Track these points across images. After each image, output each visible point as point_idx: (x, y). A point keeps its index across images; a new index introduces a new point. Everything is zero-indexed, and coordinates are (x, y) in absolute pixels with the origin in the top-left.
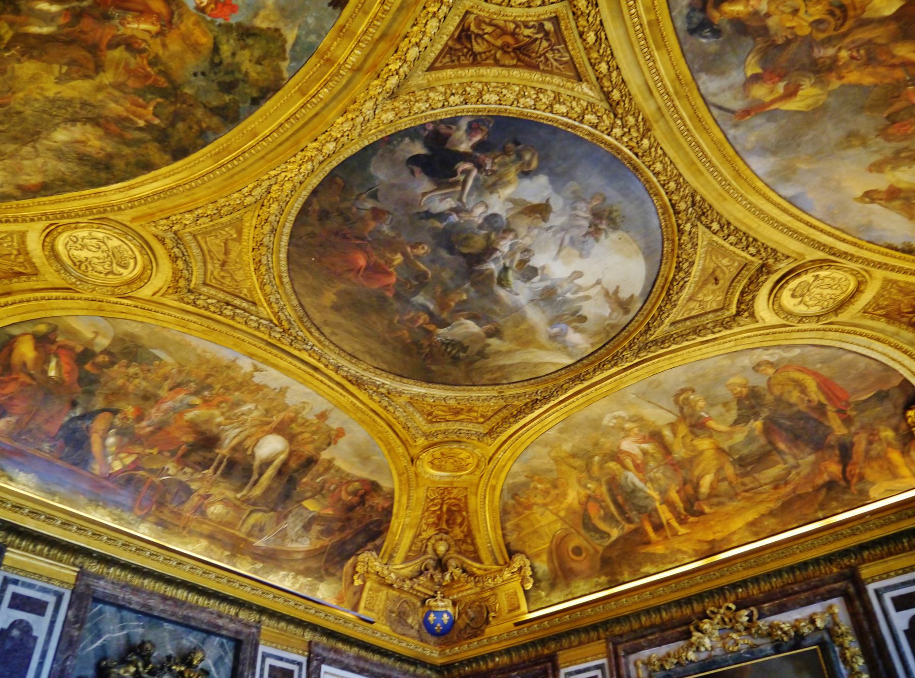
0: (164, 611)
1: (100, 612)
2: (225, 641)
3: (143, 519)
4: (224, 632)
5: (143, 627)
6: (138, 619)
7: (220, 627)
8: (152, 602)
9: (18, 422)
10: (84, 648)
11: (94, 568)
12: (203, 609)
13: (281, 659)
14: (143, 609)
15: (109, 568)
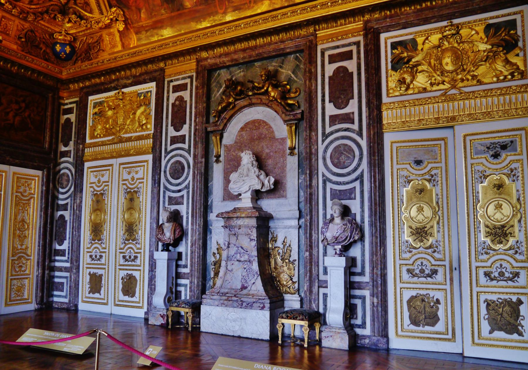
0: (244, 58)
1: (219, 74)
2: (298, 55)
3: (225, 13)
4: (288, 50)
5: (243, 71)
6: (240, 68)
7: (283, 49)
8: (236, 57)
9: (146, 10)
10: (215, 95)
11: (204, 54)
12: (270, 44)
13: (338, 47)
14: (233, 63)
15: (214, 51)
